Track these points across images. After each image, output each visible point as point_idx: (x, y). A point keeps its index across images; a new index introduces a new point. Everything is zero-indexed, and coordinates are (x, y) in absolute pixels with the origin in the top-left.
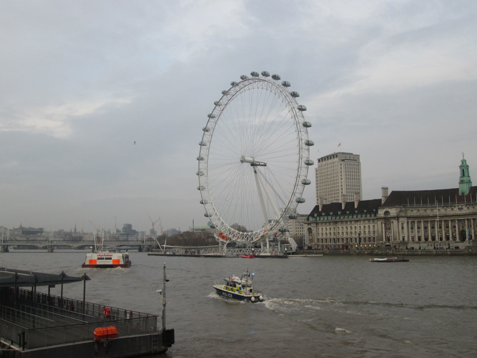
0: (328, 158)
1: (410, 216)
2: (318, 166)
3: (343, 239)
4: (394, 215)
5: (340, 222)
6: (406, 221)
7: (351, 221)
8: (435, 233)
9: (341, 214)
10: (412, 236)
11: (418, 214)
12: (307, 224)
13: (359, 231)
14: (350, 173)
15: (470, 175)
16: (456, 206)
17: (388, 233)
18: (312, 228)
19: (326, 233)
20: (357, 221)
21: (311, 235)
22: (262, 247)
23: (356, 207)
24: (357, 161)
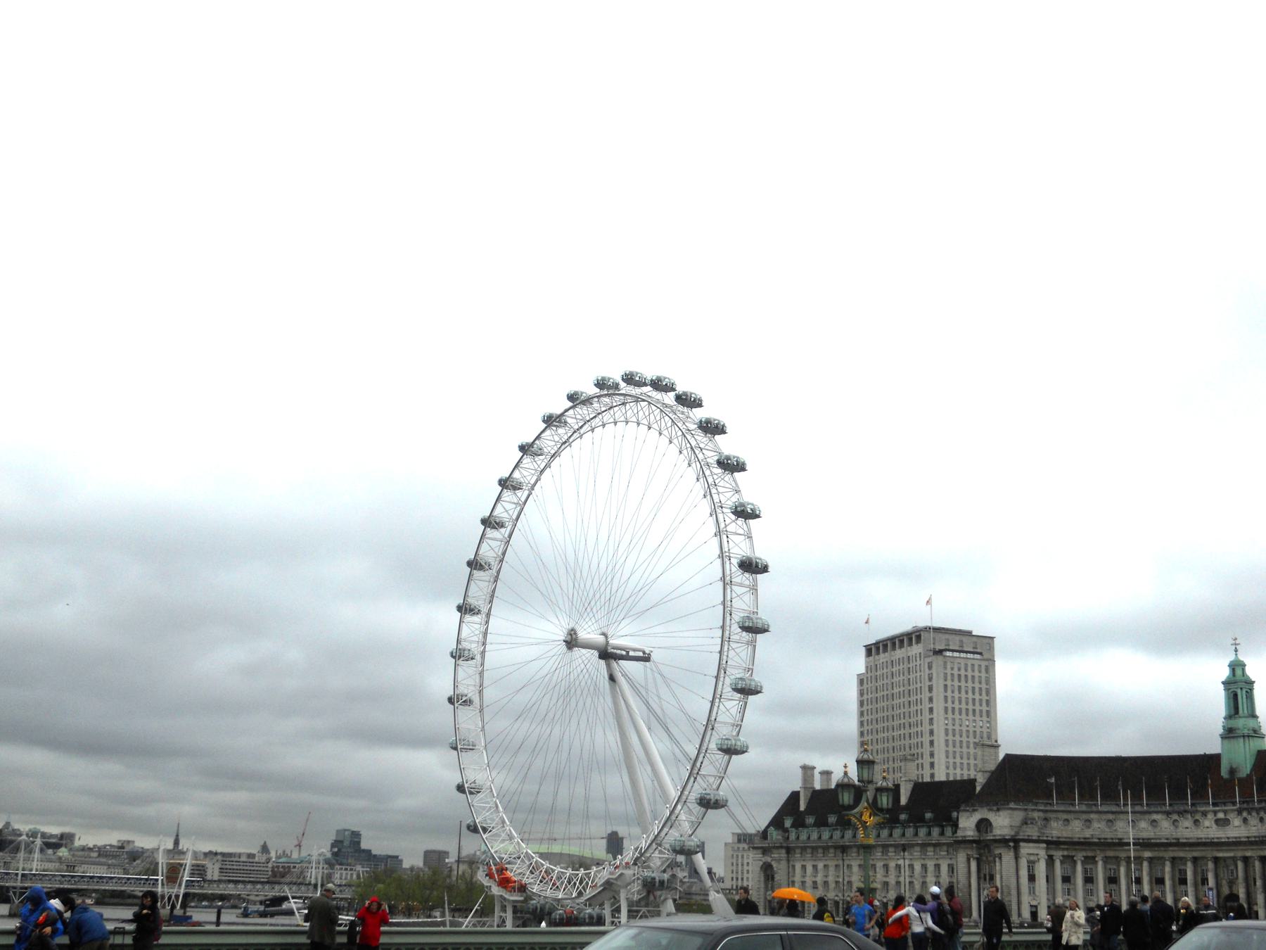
0: (894, 644)
1: (1059, 838)
2: (867, 667)
4: (1006, 833)
6: (1042, 854)
7: (885, 847)
11: (1087, 833)
12: (760, 851)
13: (907, 880)
14: (981, 695)
15: (1258, 712)
16: (1209, 811)
18: (773, 863)
19: (815, 883)
20: (904, 848)
21: (770, 886)
24: (986, 656)
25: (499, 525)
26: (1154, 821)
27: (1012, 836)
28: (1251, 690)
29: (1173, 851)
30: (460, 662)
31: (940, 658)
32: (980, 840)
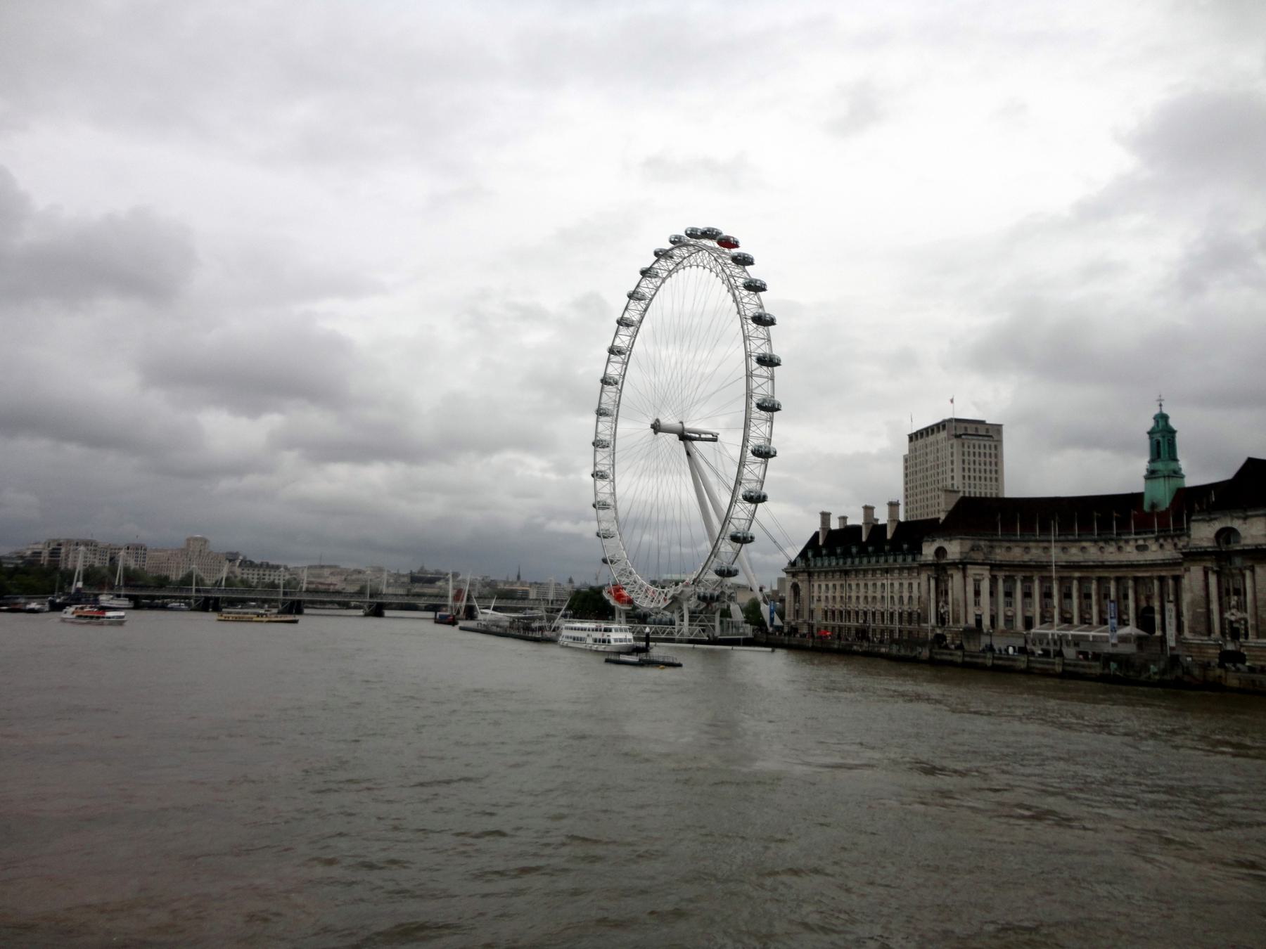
1: (1001, 561)
3: (857, 613)
5: (853, 573)
7: (874, 571)
8: (1070, 611)
9: (859, 553)
10: (1009, 616)
11: (1026, 558)
12: (790, 575)
15: (1179, 456)
17: (941, 604)
18: (800, 584)
19: (827, 597)
20: (887, 571)
21: (797, 600)
22: (677, 623)
23: (889, 536)
25: (620, 352)
26: (1083, 549)
27: (960, 559)
28: (1173, 438)
29: (1100, 572)
30: (598, 449)
31: (960, 441)
32: (938, 563)
